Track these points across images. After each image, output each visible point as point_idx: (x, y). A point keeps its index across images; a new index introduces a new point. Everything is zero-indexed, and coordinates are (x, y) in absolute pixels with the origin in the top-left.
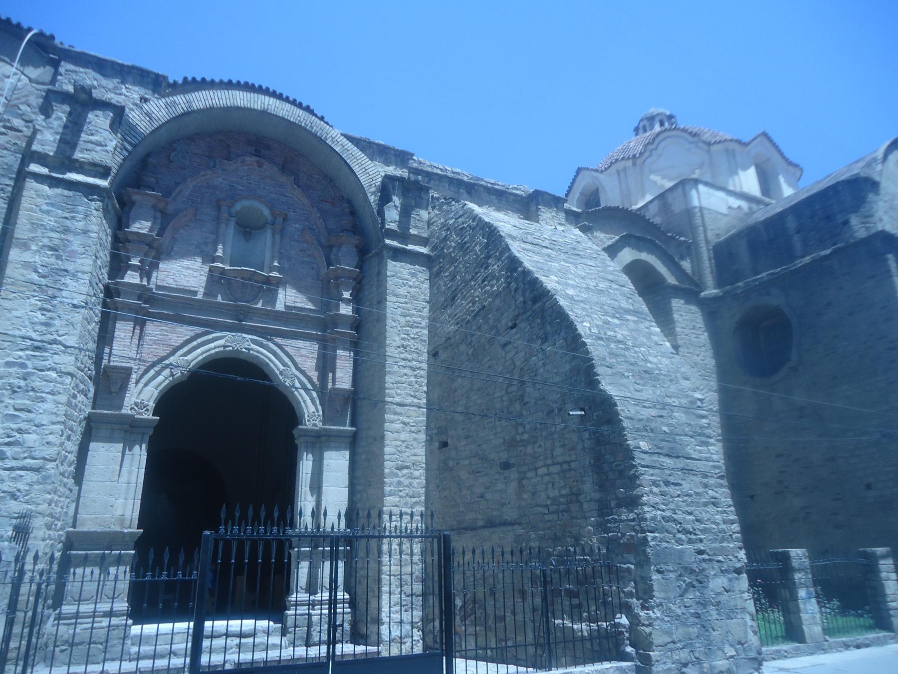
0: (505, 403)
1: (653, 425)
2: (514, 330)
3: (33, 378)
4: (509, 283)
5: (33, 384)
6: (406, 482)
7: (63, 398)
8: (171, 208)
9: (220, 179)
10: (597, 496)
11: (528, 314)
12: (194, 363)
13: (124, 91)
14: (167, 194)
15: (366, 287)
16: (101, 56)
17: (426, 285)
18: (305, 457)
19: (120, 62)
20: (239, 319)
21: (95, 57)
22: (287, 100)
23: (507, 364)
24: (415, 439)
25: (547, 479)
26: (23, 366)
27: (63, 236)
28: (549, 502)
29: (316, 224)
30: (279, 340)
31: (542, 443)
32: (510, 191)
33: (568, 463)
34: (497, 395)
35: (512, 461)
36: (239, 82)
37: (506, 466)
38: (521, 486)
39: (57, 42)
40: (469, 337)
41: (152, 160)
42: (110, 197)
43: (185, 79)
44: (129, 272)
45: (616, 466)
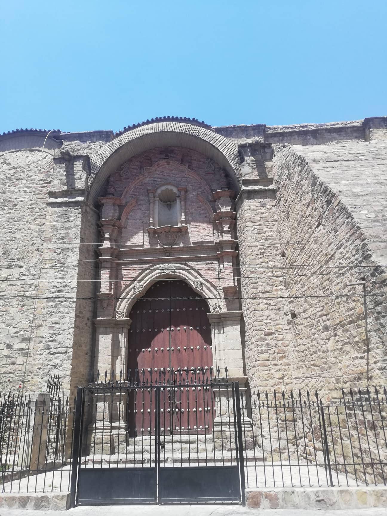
3: (59, 306)
4: (313, 196)
5: (59, 310)
6: (273, 343)
7: (73, 315)
8: (124, 202)
9: (148, 179)
13: (93, 146)
18: (213, 332)
20: (167, 254)
24: (276, 314)
27: (65, 232)
29: (205, 189)
35: (328, 323)
41: (112, 179)
43: (125, 128)
44: (105, 242)
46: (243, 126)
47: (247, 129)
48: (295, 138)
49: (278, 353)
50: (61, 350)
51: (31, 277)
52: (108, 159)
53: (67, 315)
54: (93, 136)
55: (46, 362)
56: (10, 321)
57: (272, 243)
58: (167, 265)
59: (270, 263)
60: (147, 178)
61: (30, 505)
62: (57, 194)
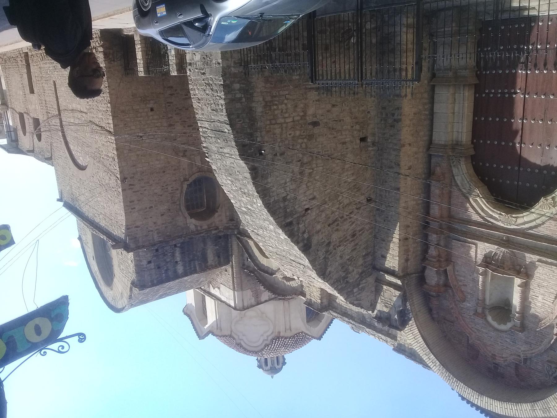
0: (314, 162)
1: (224, 143)
2: (306, 207)
10: (254, 105)
11: (295, 216)
23: (312, 187)
25: (287, 115)
28: (286, 101)
29: (456, 305)
30: (480, 220)
31: (289, 136)
32: (339, 316)
33: (271, 124)
34: (321, 168)
35: (310, 127)
37: (315, 124)
38: (305, 112)
40: (341, 207)
45: (240, 121)
46: (413, 360)
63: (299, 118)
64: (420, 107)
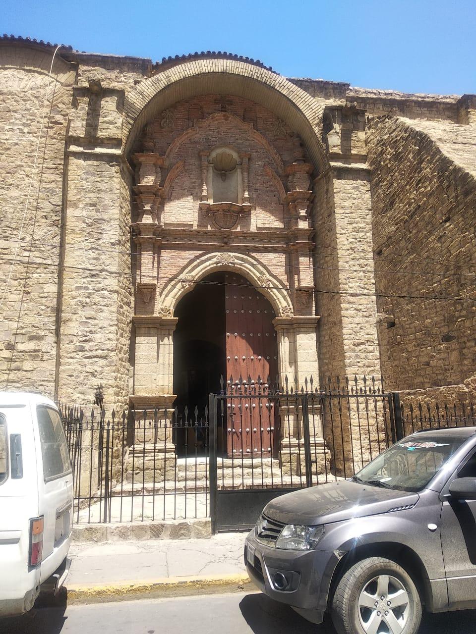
3: (94, 296)
5: (94, 301)
6: (362, 355)
7: (114, 309)
8: (167, 163)
9: (199, 135)
12: (196, 277)
14: (163, 154)
15: (318, 204)
16: (103, 55)
17: (368, 195)
18: (282, 341)
19: (117, 56)
21: (99, 56)
22: (241, 59)
23: (444, 252)
24: (367, 322)
26: (86, 288)
27: (98, 196)
29: (274, 159)
30: (254, 254)
32: (439, 101)
34: (435, 280)
35: (453, 334)
36: (203, 53)
38: (462, 356)
39: (74, 51)
41: (149, 129)
42: (124, 162)
44: (145, 216)
47: (327, 86)
48: (379, 108)
49: (367, 367)
50: (99, 352)
51: (38, 254)
52: (150, 100)
53: (105, 308)
54: (124, 64)
55: (80, 368)
56: (9, 313)
57: (365, 237)
58: (226, 254)
59: (361, 261)
60: (197, 134)
61: (165, 534)
62: (81, 140)
63: (469, 344)
64: (330, 367)
